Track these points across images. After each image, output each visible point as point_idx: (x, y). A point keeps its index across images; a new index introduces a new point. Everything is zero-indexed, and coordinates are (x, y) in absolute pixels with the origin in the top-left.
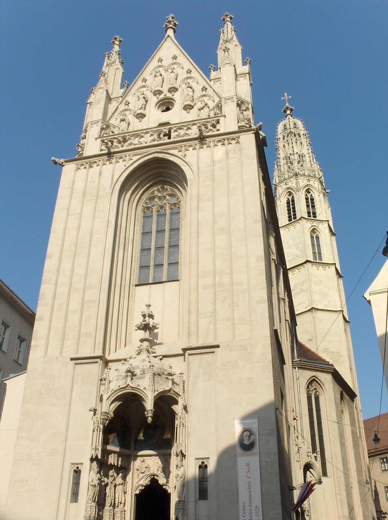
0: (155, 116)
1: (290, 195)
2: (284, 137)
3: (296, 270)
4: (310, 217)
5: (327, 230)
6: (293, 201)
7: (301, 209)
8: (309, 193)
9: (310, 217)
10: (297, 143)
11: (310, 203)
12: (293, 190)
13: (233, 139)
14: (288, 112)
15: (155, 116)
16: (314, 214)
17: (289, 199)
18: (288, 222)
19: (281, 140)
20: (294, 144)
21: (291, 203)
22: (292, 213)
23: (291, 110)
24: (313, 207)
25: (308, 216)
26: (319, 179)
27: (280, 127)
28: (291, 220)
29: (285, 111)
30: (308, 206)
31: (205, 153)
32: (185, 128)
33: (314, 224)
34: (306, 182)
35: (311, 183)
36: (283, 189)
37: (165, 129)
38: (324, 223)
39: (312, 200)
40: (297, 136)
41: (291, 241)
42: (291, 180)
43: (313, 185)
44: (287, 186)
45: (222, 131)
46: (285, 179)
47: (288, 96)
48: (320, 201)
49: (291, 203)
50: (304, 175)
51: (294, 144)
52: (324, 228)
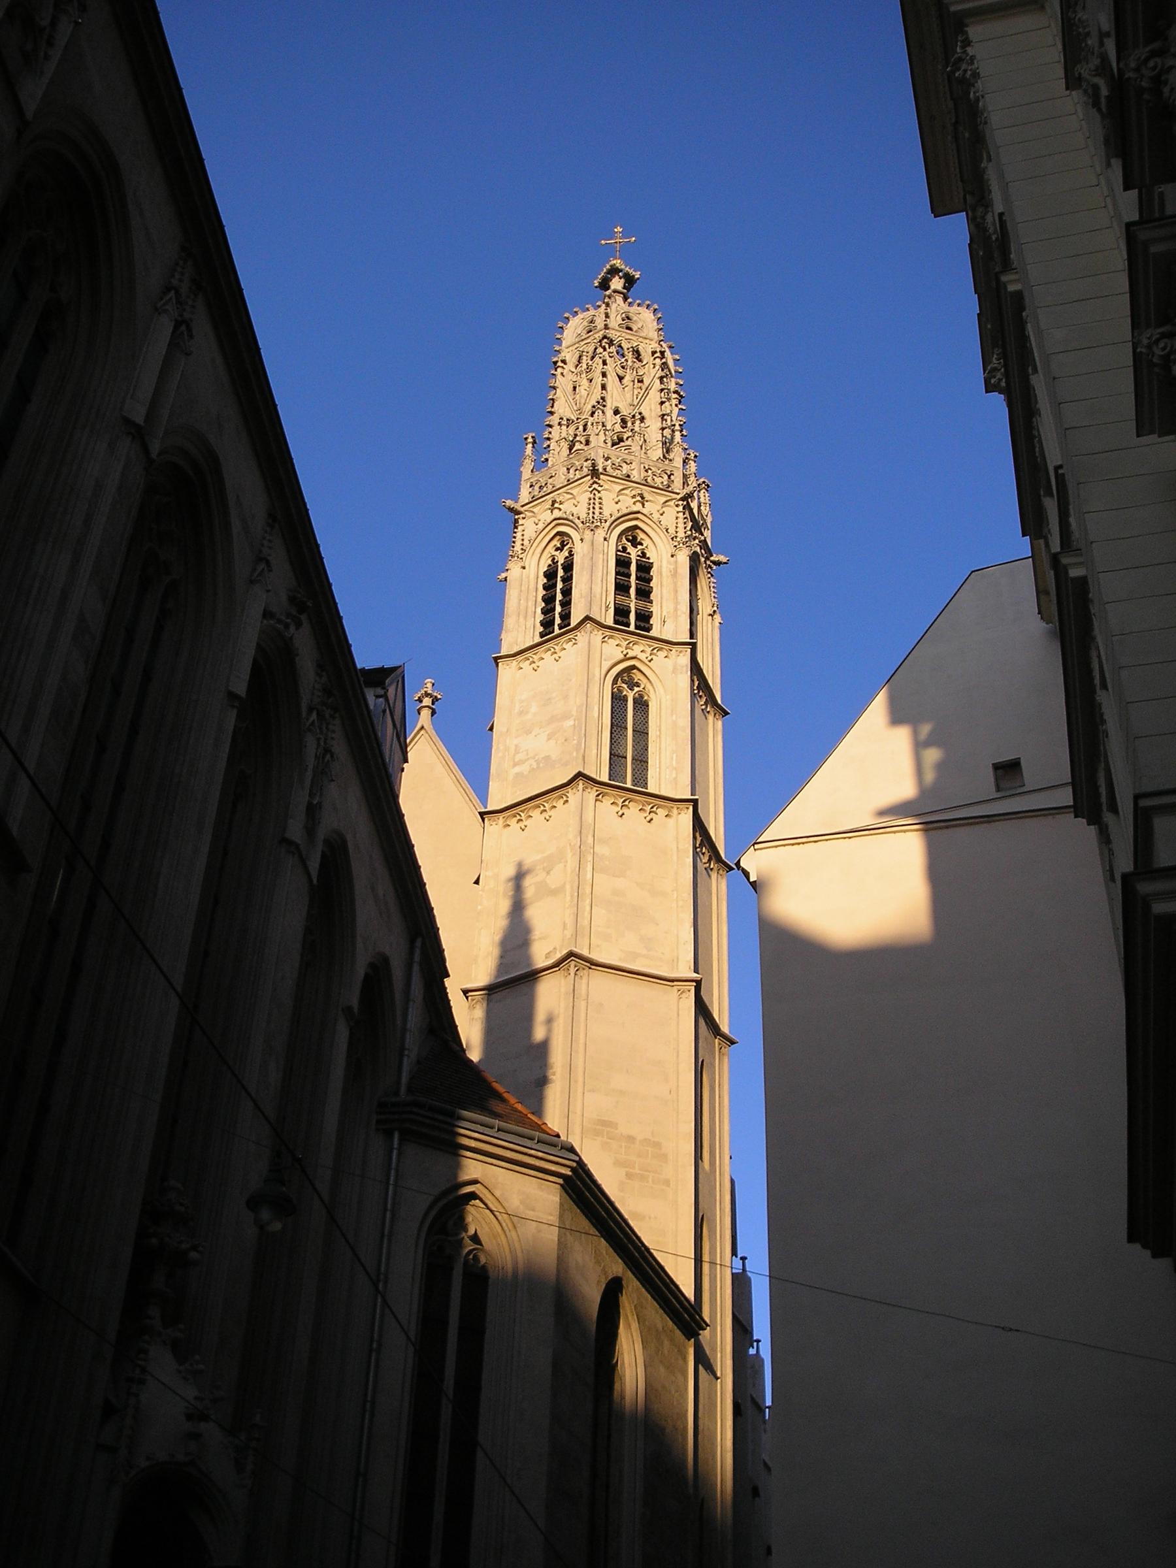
1: (560, 549)
3: (536, 813)
5: (684, 681)
6: (568, 567)
7: (594, 590)
8: (635, 542)
9: (628, 625)
10: (621, 378)
11: (634, 577)
12: (577, 529)
14: (617, 283)
16: (644, 619)
17: (554, 562)
18: (538, 639)
19: (570, 366)
20: (612, 380)
21: (561, 573)
22: (558, 609)
23: (630, 281)
24: (644, 593)
25: (616, 622)
26: (688, 497)
27: (574, 327)
29: (605, 285)
30: (621, 588)
33: (636, 651)
34: (628, 503)
36: (541, 526)
38: (675, 648)
39: (645, 569)
40: (629, 356)
41: (534, 709)
42: (574, 492)
44: (557, 514)
47: (625, 234)
48: (675, 574)
49: (561, 573)
51: (612, 380)
52: (675, 671)
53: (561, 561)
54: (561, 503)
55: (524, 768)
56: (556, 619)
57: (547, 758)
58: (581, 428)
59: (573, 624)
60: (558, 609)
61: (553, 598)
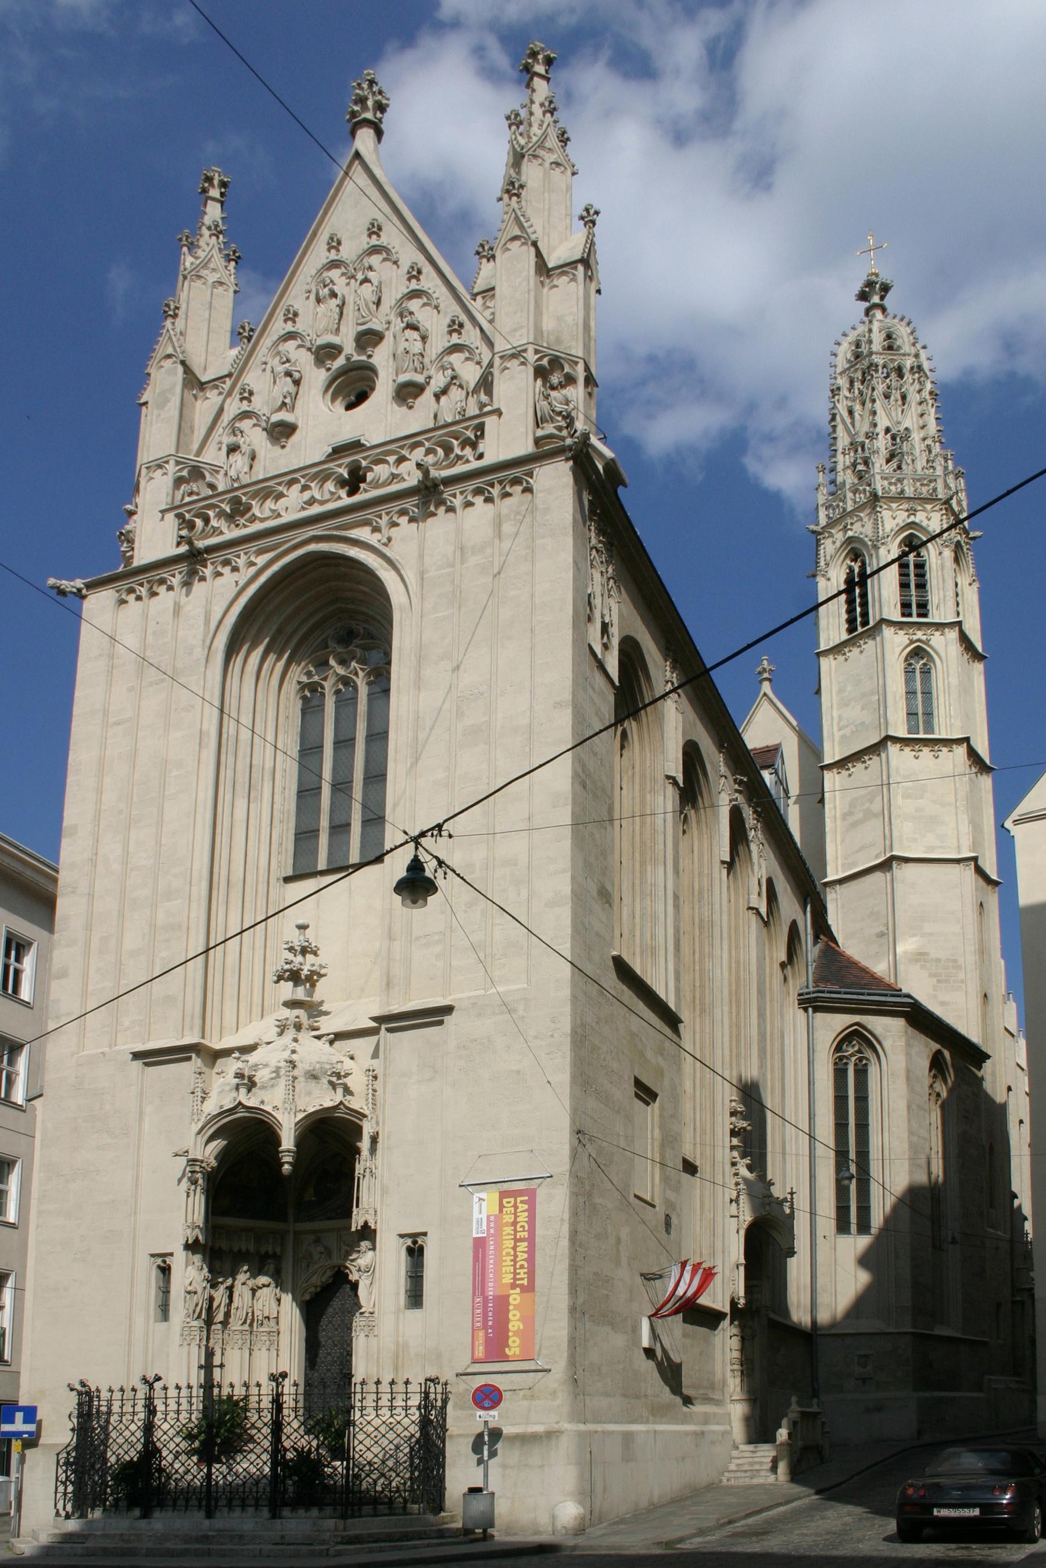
0: (323, 424)
2: (852, 383)
4: (910, 615)
13: (516, 481)
15: (323, 424)
18: (845, 636)
22: (858, 609)
24: (921, 586)
25: (903, 615)
28: (856, 629)
31: (439, 525)
32: (392, 459)
34: (902, 518)
35: (920, 518)
36: (838, 544)
37: (340, 466)
40: (893, 375)
41: (849, 688)
43: (924, 524)
44: (850, 533)
45: (488, 460)
46: (845, 514)
50: (900, 497)
53: (857, 570)
54: (852, 524)
55: (847, 732)
56: (861, 624)
57: (862, 724)
58: (860, 449)
59: (872, 623)
60: (858, 609)
61: (855, 619)
